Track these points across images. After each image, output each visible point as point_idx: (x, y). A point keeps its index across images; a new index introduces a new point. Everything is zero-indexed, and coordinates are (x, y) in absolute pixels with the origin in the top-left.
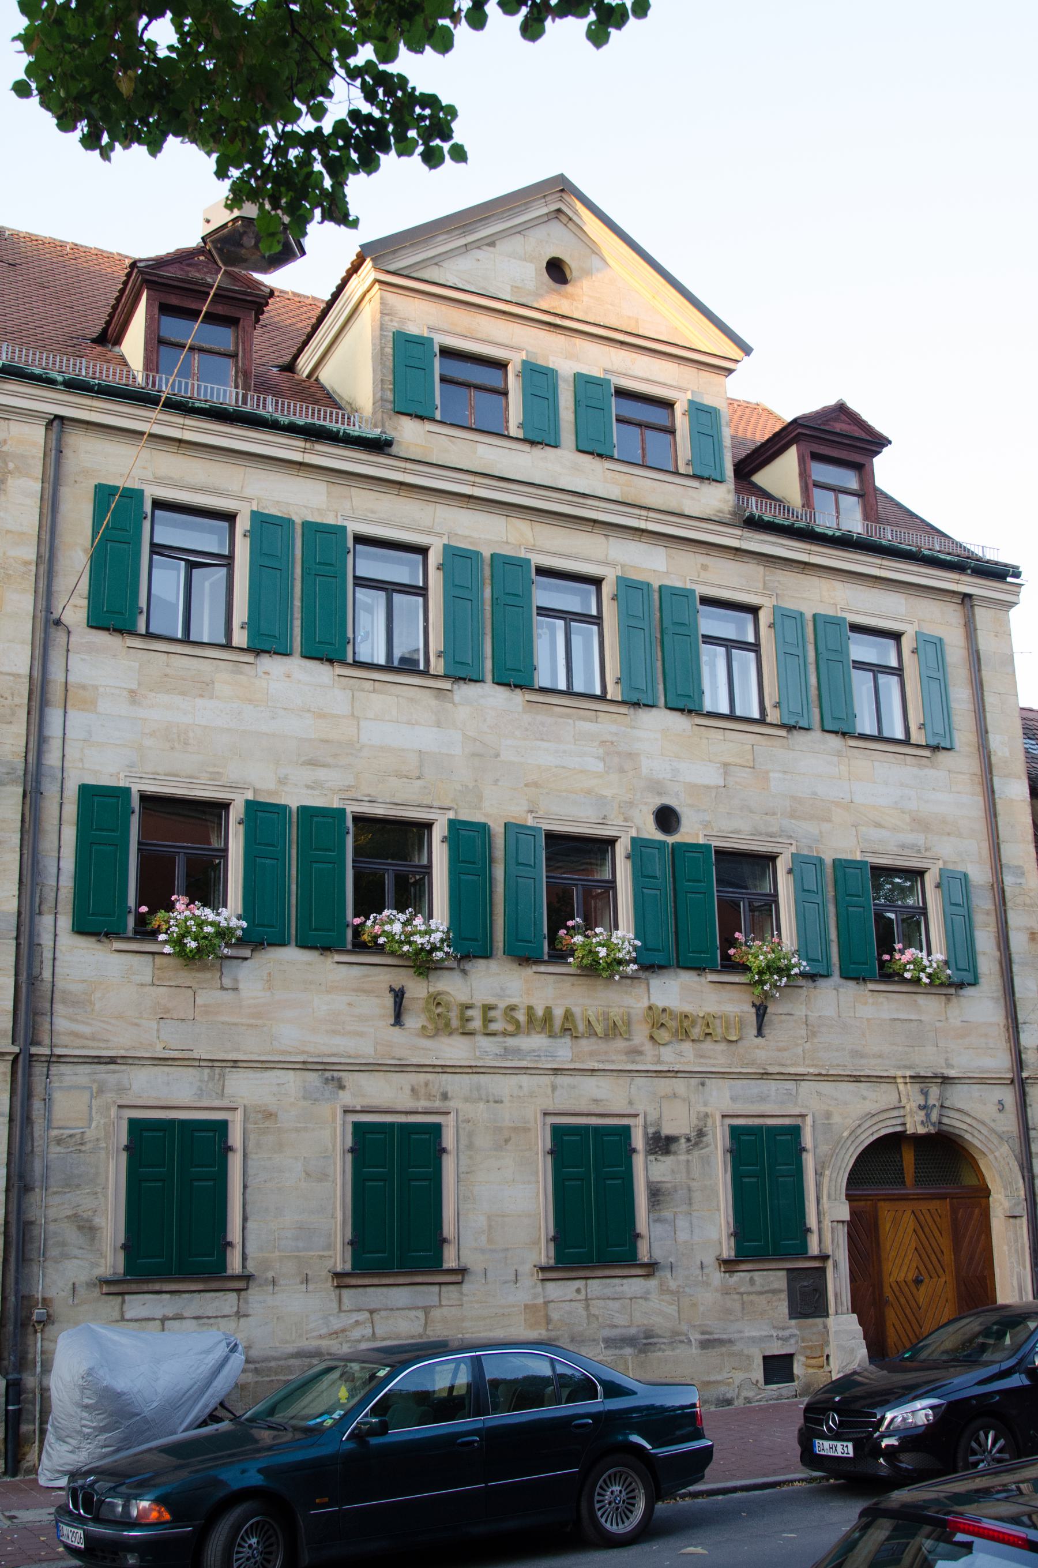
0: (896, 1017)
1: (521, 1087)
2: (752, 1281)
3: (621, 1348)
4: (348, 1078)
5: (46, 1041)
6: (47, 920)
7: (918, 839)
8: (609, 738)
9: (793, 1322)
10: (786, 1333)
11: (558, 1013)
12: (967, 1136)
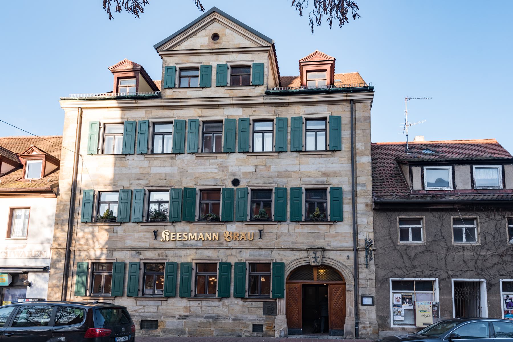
2: (252, 304)
4: (142, 252)
7: (325, 179)
10: (261, 319)
12: (334, 267)
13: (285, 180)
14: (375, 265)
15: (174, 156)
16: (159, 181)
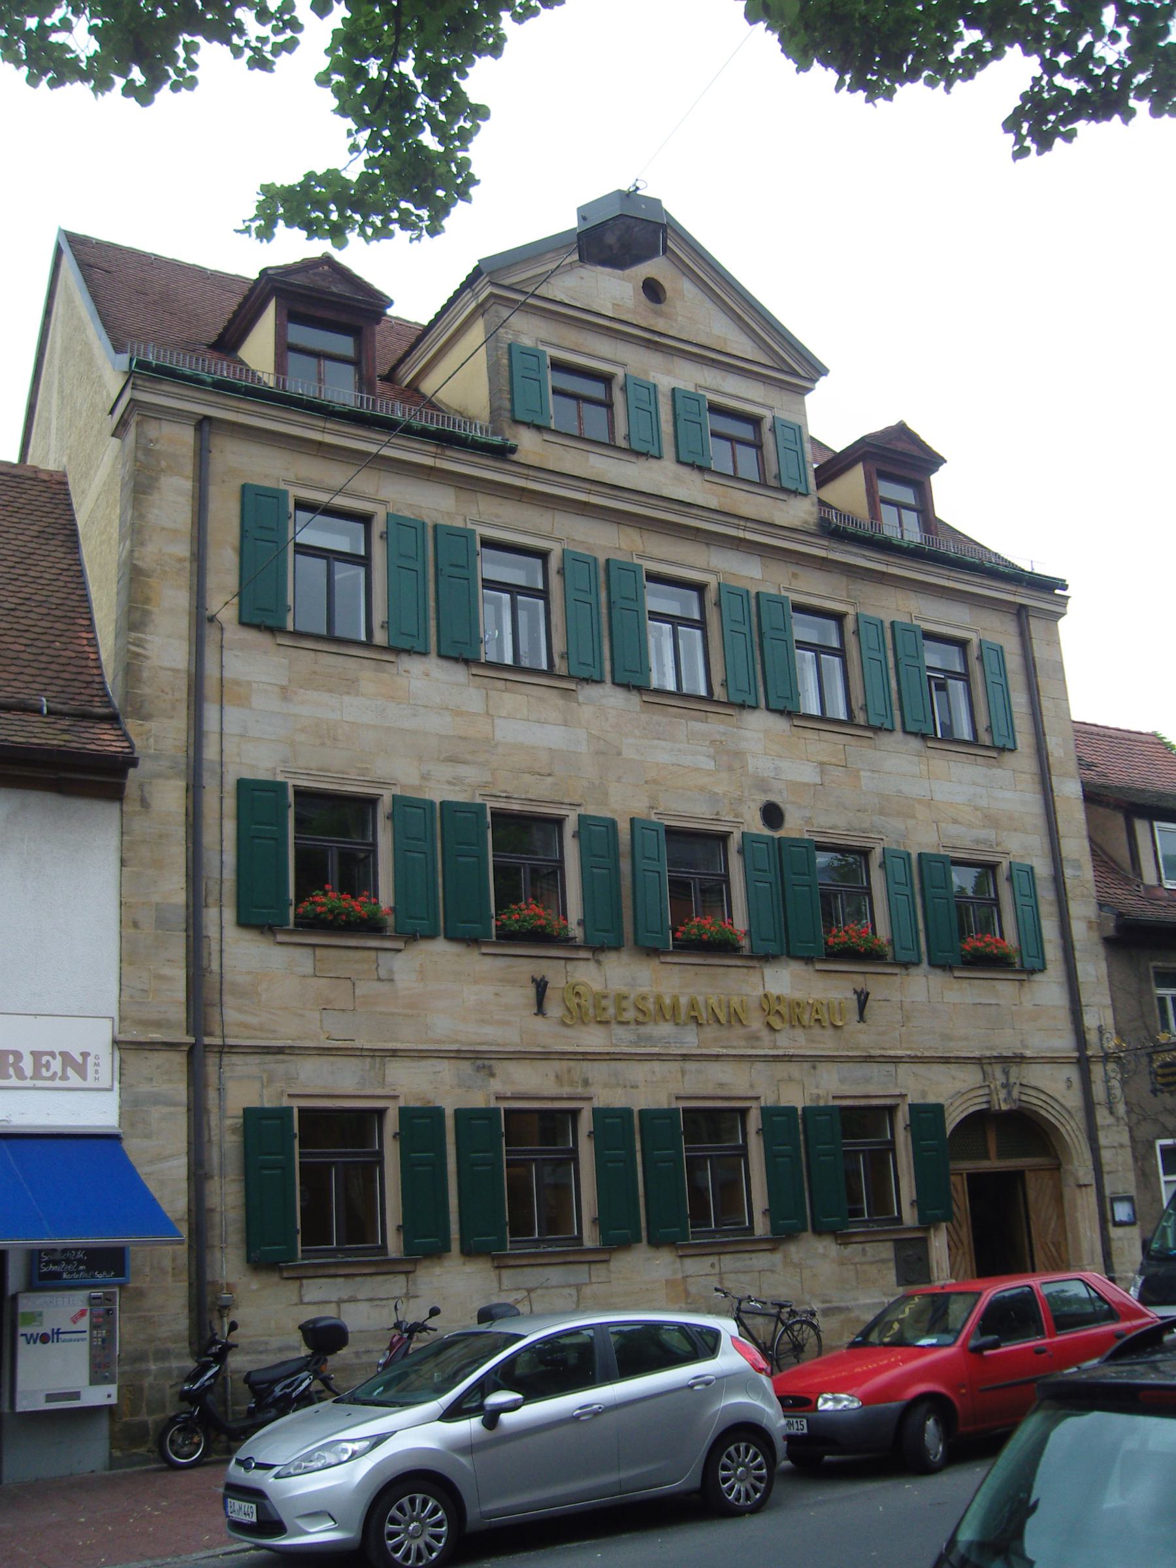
0: (978, 1001)
1: (653, 1072)
2: (864, 1251)
5: (217, 1030)
7: (989, 834)
8: (717, 737)
11: (683, 1001)
13: (897, 824)
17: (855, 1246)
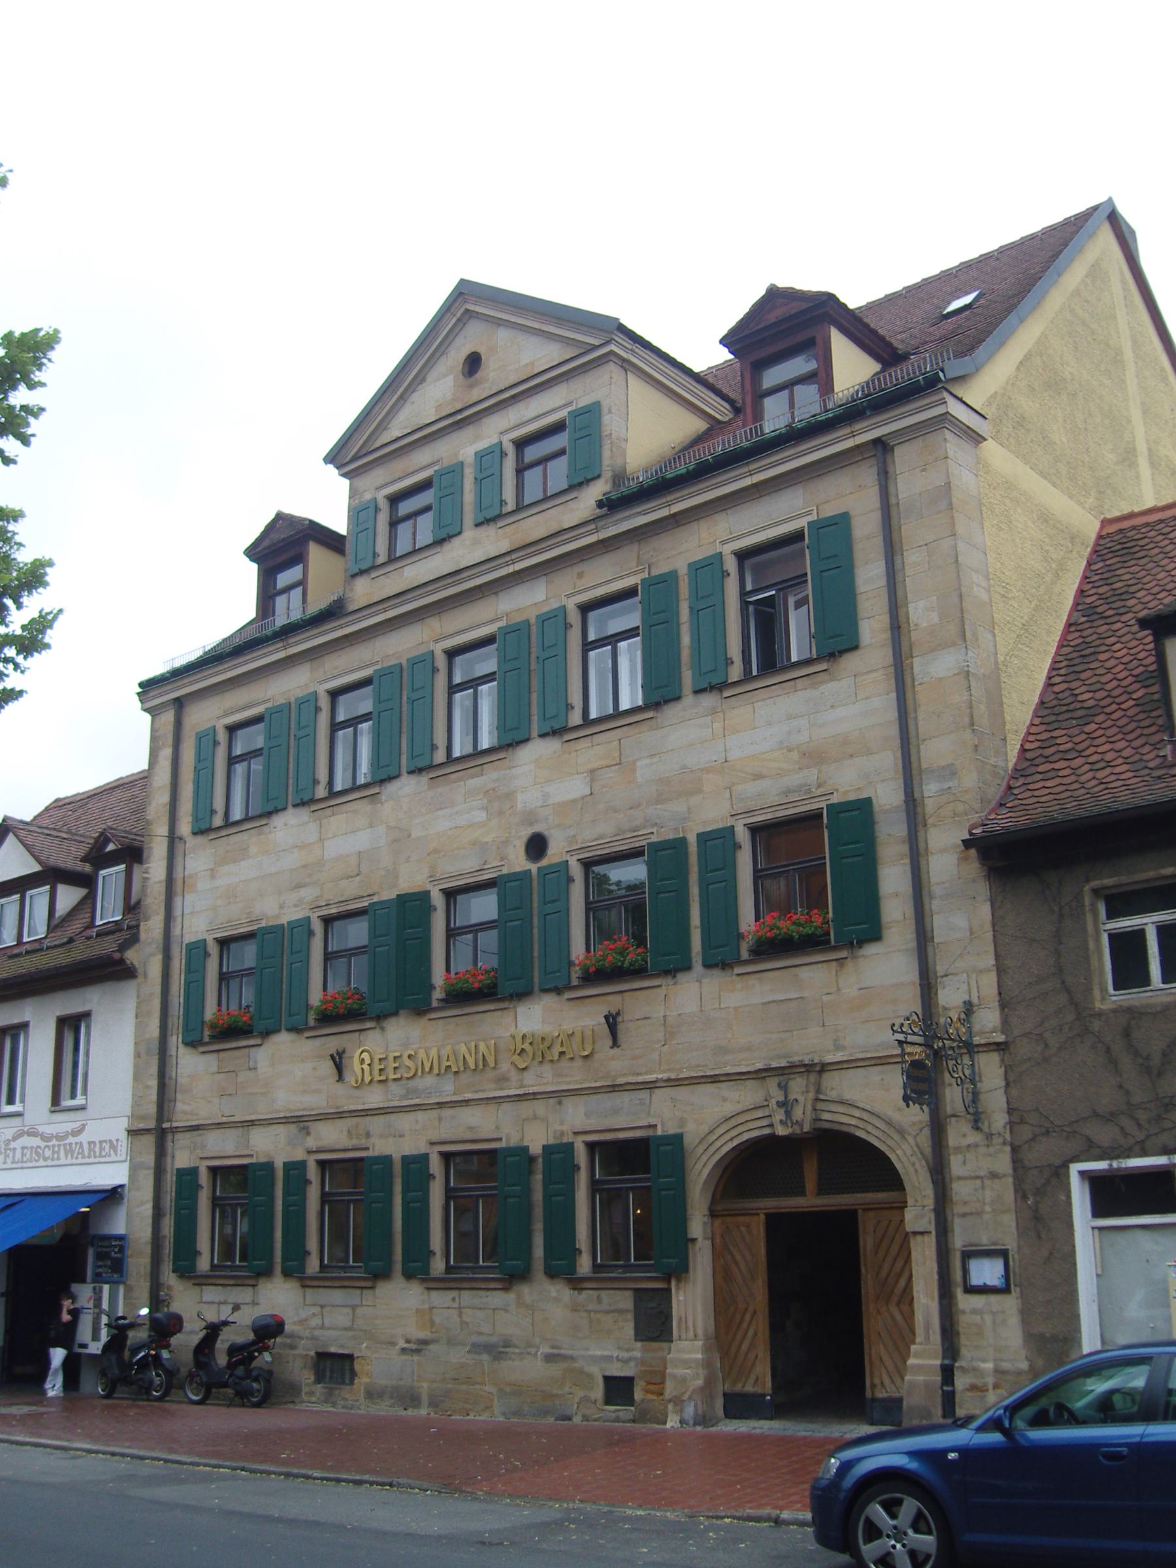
3: (480, 1353)
6: (175, 1037)
7: (811, 775)
8: (490, 786)
9: (639, 1344)
10: (626, 1355)
13: (678, 807)
14: (1010, 1111)
15: (376, 790)
16: (344, 883)
17: (590, 1292)
